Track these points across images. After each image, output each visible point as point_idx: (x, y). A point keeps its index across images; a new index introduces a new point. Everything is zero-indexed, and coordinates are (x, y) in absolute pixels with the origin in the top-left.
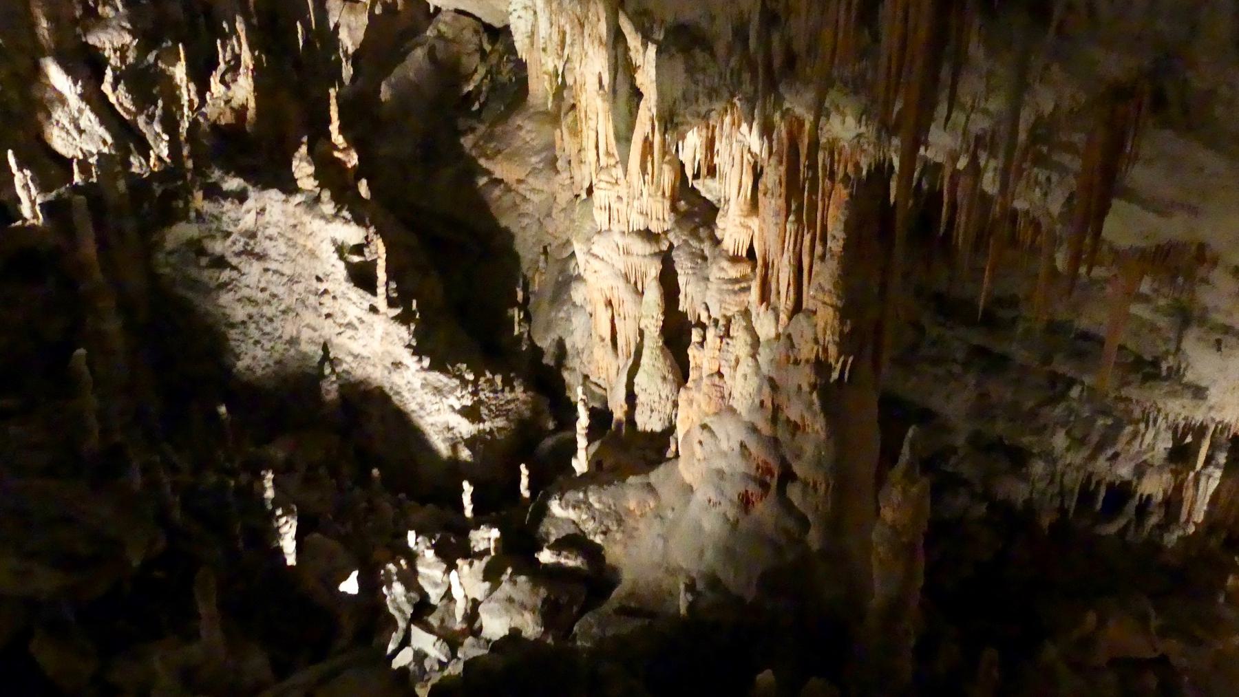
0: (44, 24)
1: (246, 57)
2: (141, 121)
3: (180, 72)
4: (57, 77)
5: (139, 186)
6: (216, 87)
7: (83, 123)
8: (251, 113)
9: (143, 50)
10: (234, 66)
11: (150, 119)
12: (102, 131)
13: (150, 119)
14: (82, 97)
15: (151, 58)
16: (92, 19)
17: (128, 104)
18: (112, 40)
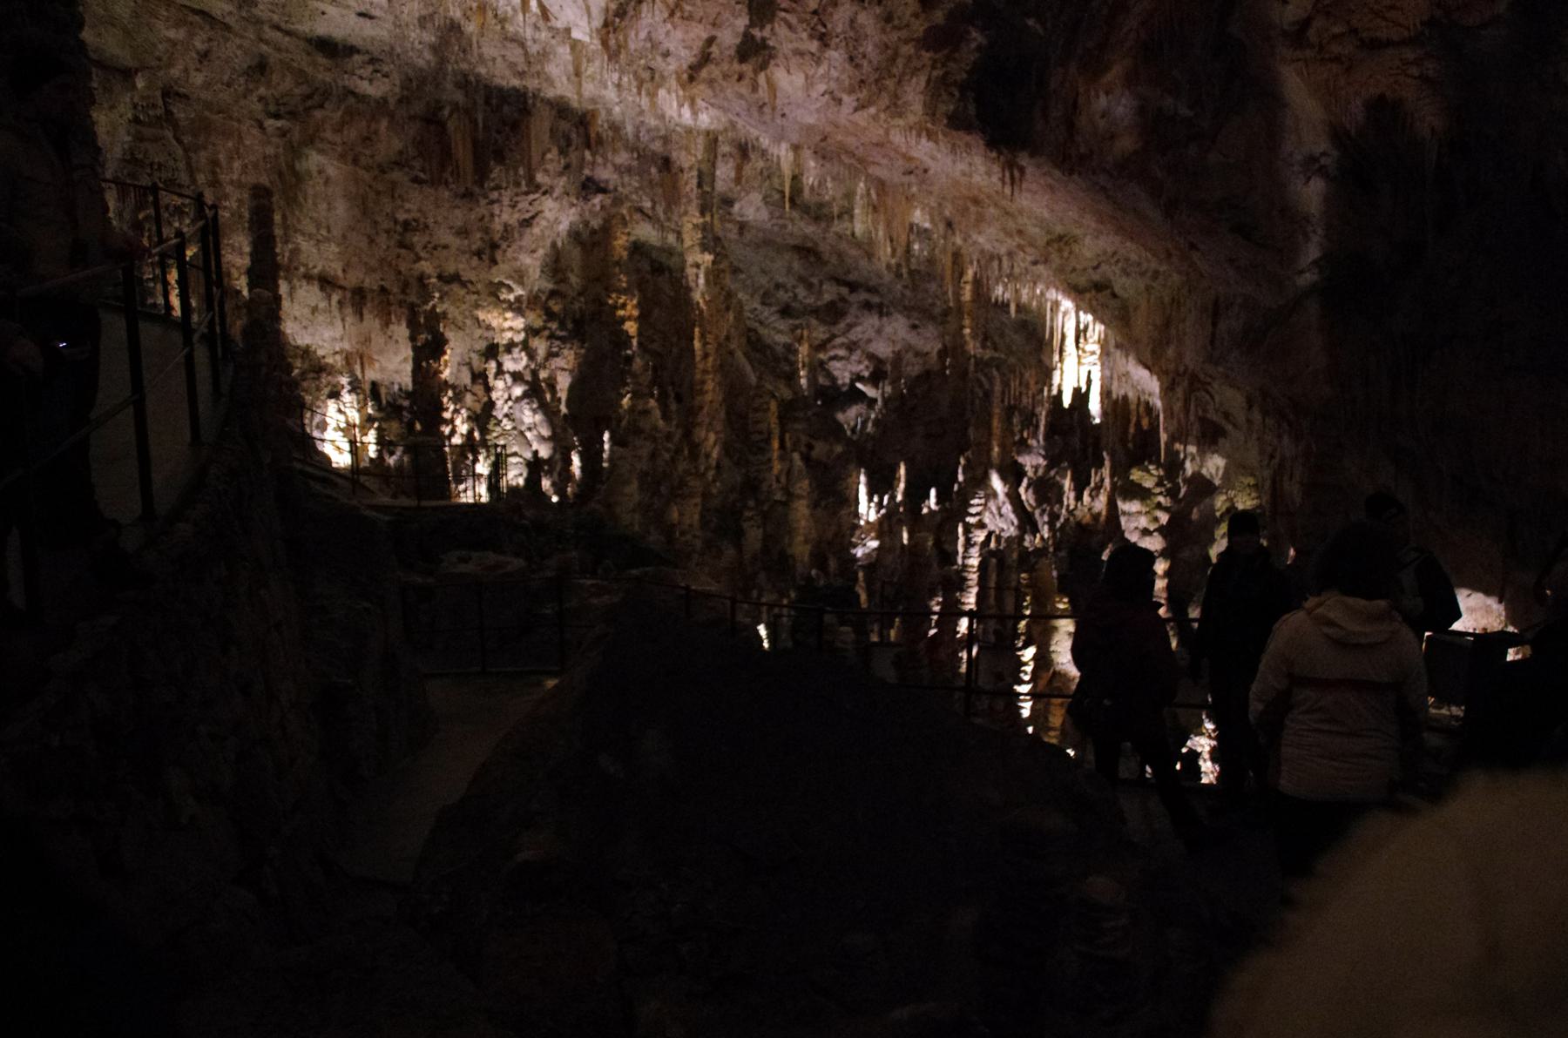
0: (996, 449)
1: (1107, 481)
2: (1037, 512)
3: (1067, 483)
4: (997, 483)
5: (1025, 555)
6: (1086, 498)
7: (1004, 510)
8: (1103, 518)
9: (1048, 468)
10: (1098, 487)
11: (1043, 511)
12: (1012, 516)
13: (1043, 511)
14: (1007, 495)
15: (1052, 473)
16: (1023, 447)
17: (1032, 502)
18: (1031, 462)
